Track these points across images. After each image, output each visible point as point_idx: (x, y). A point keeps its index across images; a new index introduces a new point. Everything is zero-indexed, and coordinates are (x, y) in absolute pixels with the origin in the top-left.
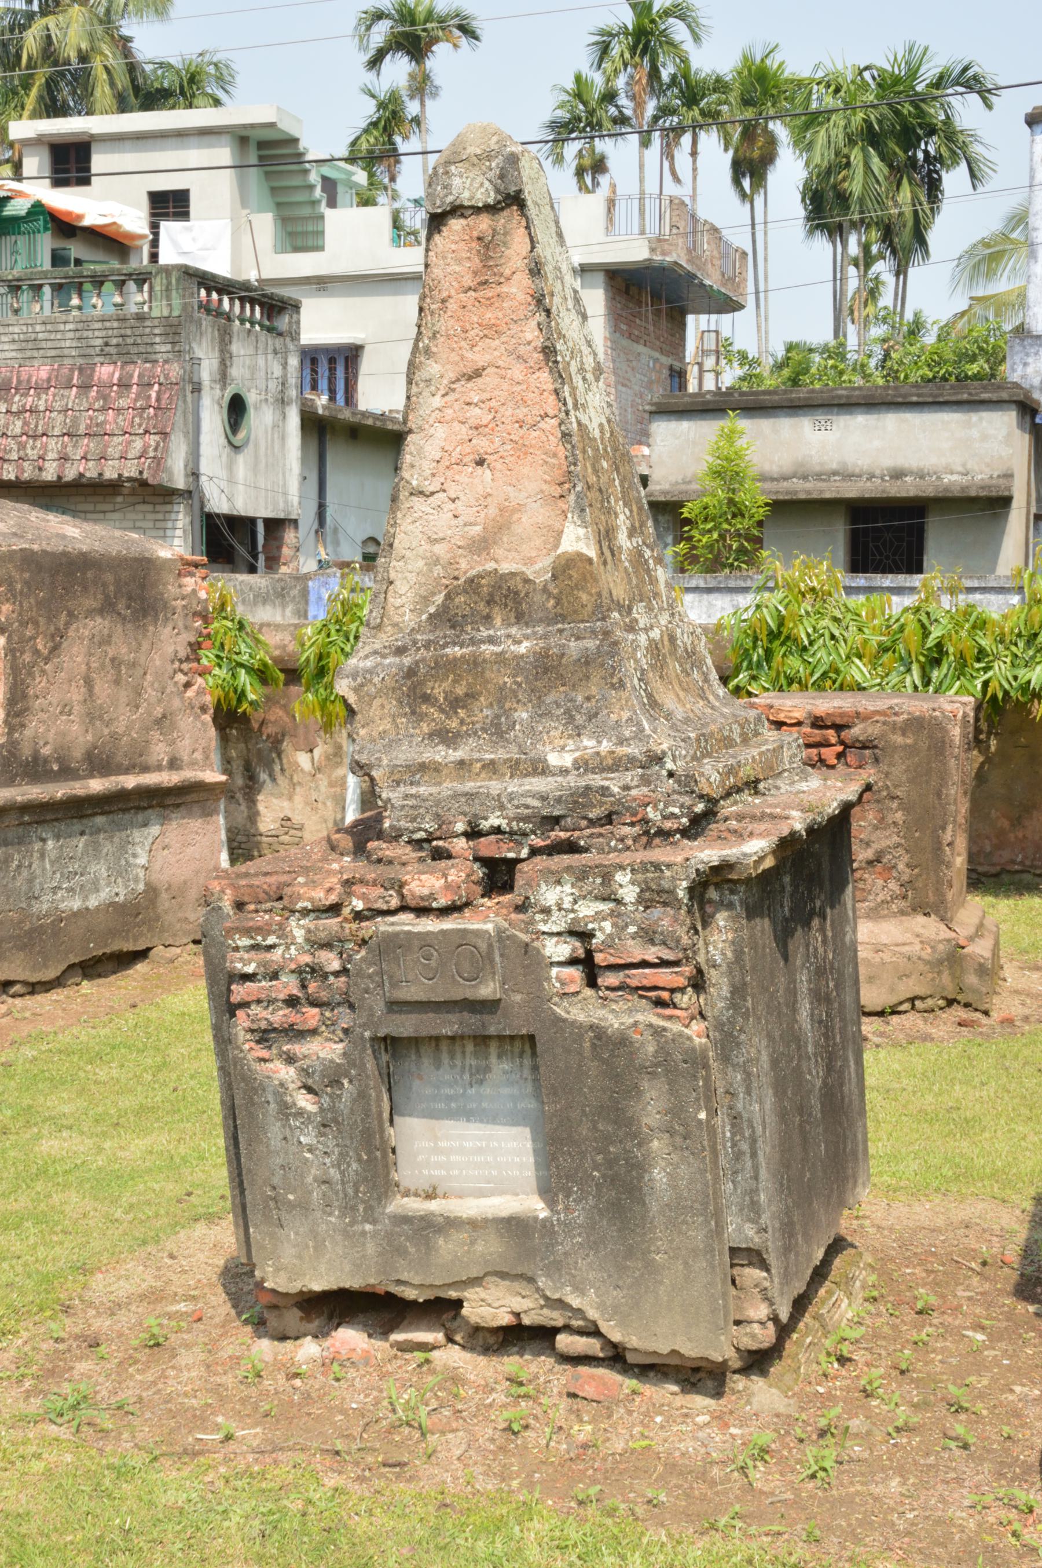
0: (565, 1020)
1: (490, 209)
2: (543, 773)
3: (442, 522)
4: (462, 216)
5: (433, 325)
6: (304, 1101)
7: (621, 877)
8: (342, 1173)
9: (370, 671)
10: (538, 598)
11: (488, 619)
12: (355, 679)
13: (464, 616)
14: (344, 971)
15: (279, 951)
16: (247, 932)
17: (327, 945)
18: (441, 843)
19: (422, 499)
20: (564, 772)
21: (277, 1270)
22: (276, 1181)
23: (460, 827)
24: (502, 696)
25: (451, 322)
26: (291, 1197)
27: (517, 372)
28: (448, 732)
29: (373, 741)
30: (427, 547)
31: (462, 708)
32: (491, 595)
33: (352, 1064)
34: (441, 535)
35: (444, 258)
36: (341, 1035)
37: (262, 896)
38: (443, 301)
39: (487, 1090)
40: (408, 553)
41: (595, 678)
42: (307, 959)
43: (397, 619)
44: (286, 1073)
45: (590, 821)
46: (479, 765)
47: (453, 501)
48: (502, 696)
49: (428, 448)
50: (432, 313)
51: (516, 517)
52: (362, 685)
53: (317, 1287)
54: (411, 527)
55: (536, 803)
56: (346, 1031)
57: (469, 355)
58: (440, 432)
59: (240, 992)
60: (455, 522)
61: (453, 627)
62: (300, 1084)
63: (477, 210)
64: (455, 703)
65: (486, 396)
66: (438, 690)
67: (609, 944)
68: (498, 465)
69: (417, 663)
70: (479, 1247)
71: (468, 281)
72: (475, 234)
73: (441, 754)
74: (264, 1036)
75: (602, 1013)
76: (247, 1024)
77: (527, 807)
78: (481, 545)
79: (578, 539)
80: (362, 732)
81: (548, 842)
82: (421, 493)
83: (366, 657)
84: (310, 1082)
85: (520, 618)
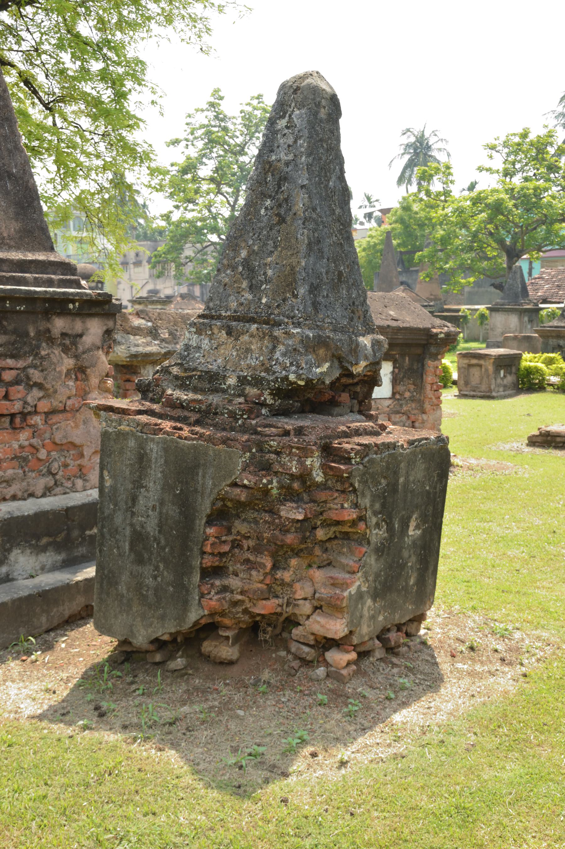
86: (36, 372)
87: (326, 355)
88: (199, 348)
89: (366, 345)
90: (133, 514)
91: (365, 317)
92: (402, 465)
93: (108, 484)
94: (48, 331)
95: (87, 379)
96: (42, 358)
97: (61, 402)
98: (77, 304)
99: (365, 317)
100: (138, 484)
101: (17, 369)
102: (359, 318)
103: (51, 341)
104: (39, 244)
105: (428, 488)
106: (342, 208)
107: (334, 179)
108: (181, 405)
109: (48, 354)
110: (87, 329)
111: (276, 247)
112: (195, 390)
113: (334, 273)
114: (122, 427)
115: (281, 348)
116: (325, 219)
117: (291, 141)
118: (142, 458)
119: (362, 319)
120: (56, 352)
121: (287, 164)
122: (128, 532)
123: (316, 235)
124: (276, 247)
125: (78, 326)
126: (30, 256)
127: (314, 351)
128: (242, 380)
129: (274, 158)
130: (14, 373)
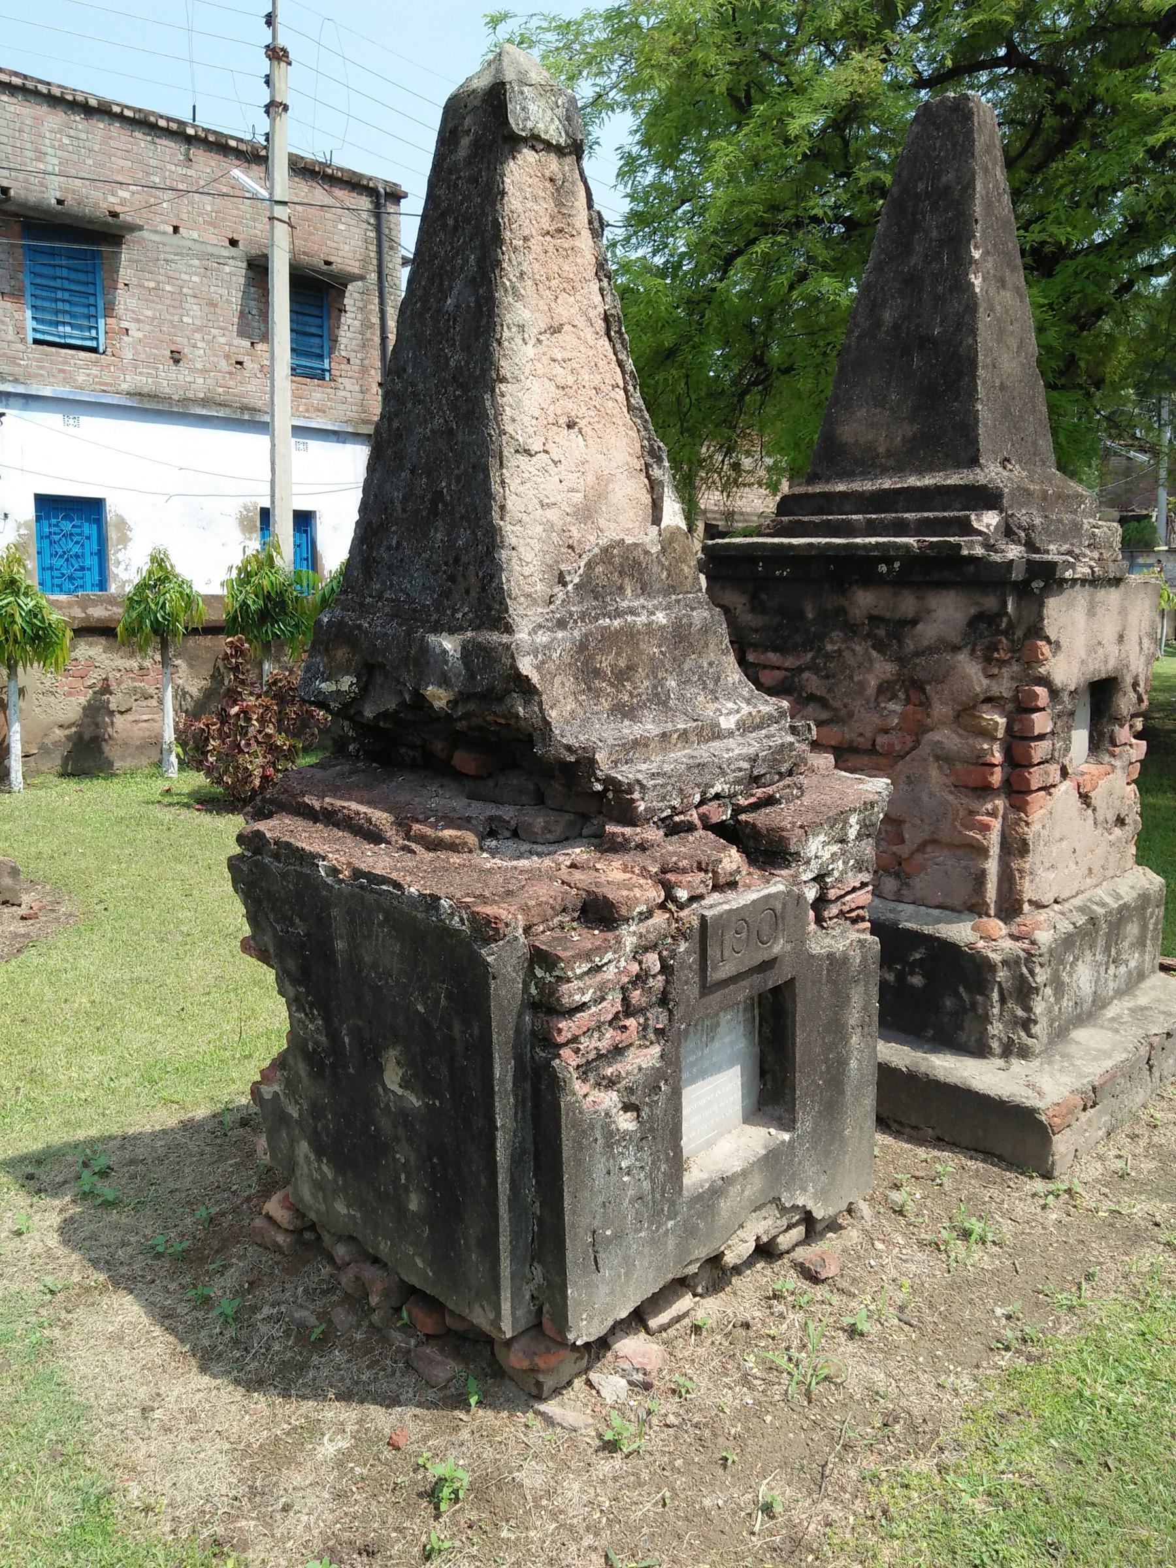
0: (813, 956)
1: (559, 150)
2: (718, 737)
3: (551, 487)
4: (533, 148)
5: (520, 264)
6: (626, 1123)
7: (853, 819)
8: (653, 1181)
9: (547, 647)
10: (656, 569)
11: (621, 588)
12: (536, 657)
13: (603, 587)
14: (666, 969)
15: (612, 967)
16: (587, 956)
17: (653, 947)
18: (682, 817)
19: (527, 458)
20: (731, 734)
21: (590, 1319)
22: (596, 1223)
23: (697, 798)
24: (654, 667)
25: (536, 266)
26: (608, 1233)
27: (588, 334)
28: (624, 705)
29: (567, 722)
30: (540, 511)
31: (628, 680)
32: (622, 565)
33: (668, 1065)
34: (553, 500)
35: (521, 190)
36: (652, 1036)
37: (550, 912)
38: (526, 239)
39: (717, 1044)
40: (525, 517)
41: (711, 647)
42: (635, 968)
43: (527, 589)
44: (609, 1100)
45: (780, 774)
46: (675, 736)
47: (555, 463)
48: (654, 667)
49: (526, 402)
50: (515, 250)
51: (611, 486)
52: (543, 663)
53: (624, 1314)
54: (521, 489)
55: (746, 765)
56: (660, 1033)
57: (553, 305)
58: (536, 385)
59: (567, 1028)
60: (561, 486)
61: (596, 598)
62: (620, 1105)
63: (549, 146)
64: (622, 676)
65: (567, 355)
66: (605, 662)
67: (838, 880)
68: (587, 430)
69: (586, 635)
70: (747, 1193)
71: (546, 223)
72: (548, 174)
73: (631, 730)
74: (585, 1070)
75: (828, 941)
76: (574, 1061)
77: (740, 770)
78: (586, 513)
79: (675, 514)
80: (554, 713)
81: (752, 800)
82: (527, 452)
83: (534, 631)
84: (633, 1099)
85: (645, 589)
86: (814, 677)
87: (349, 661)
89: (445, 652)
91: (483, 589)
92: (335, 912)
94: (842, 611)
95: (926, 704)
96: (828, 657)
97: (861, 735)
98: (897, 565)
99: (483, 589)
101: (786, 669)
102: (467, 592)
103: (852, 630)
104: (947, 456)
105: (421, 1008)
106: (466, 348)
107: (458, 285)
109: (839, 651)
110: (929, 612)
113: (422, 498)
116: (421, 386)
119: (474, 594)
120: (857, 648)
123: (395, 425)
125: (908, 605)
126: (913, 481)
127: (327, 650)
130: (779, 675)
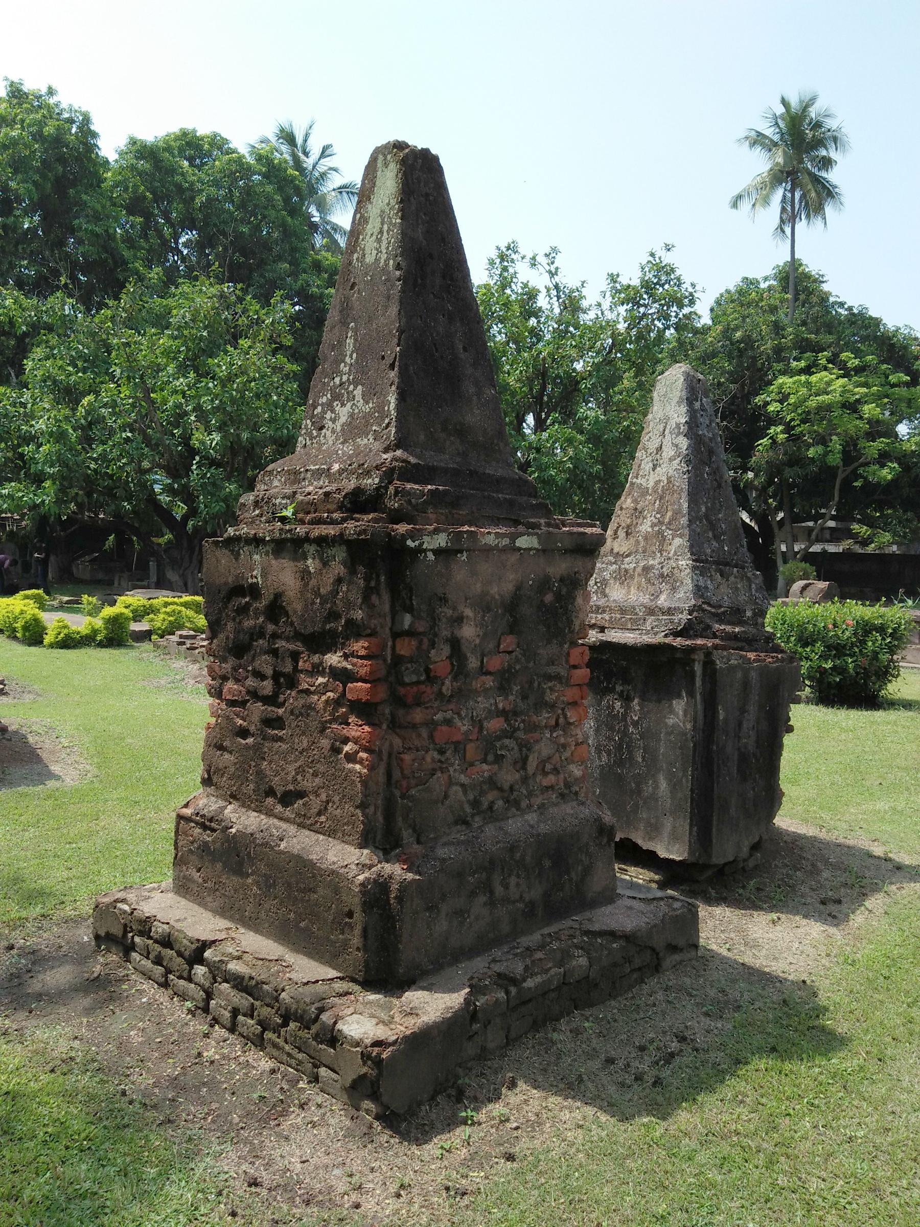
88: (706, 588)
90: (739, 737)
93: (721, 718)
100: (743, 710)
108: (734, 637)
111: (721, 506)
112: (729, 623)
114: (732, 662)
115: (753, 586)
117: (707, 422)
118: (746, 685)
121: (711, 439)
122: (736, 757)
124: (721, 506)
128: (755, 614)
129: (701, 432)
